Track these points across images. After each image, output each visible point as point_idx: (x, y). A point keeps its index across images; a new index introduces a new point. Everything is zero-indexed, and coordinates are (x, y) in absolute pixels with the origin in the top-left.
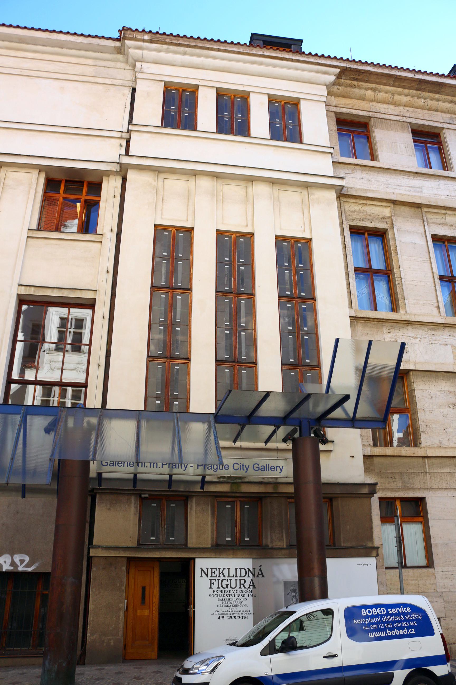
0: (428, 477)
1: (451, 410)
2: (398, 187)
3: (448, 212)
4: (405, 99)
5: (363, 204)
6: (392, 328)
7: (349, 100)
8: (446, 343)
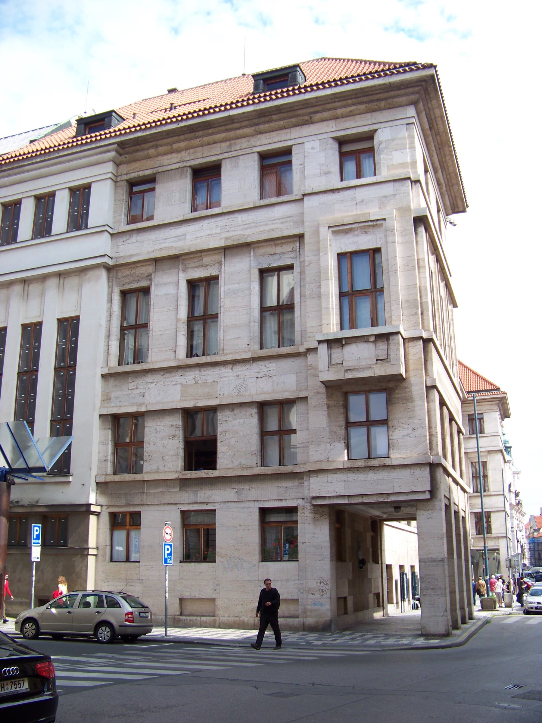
0: (145, 496)
1: (171, 441)
2: (165, 241)
3: (203, 254)
4: (182, 145)
5: (132, 268)
6: (136, 377)
7: (138, 162)
8: (177, 383)
